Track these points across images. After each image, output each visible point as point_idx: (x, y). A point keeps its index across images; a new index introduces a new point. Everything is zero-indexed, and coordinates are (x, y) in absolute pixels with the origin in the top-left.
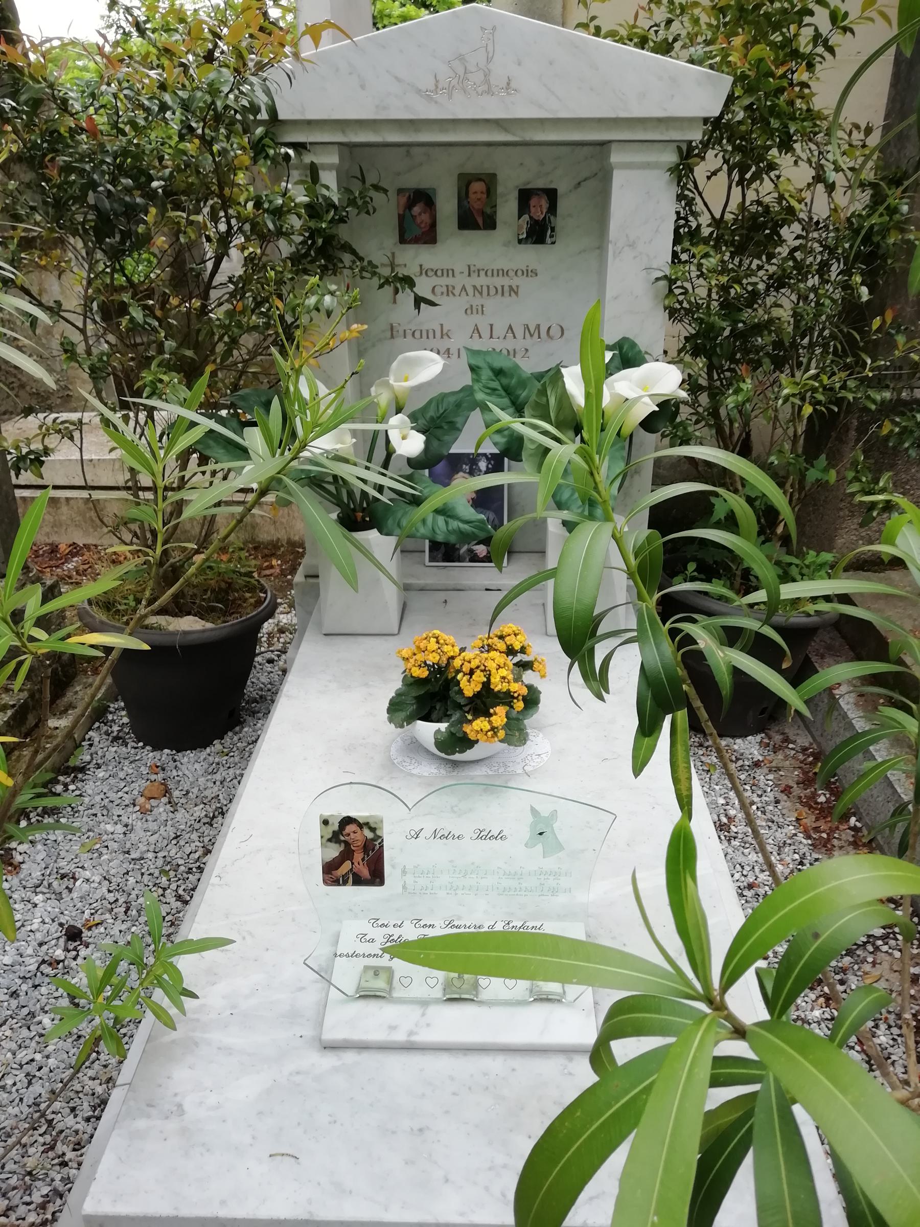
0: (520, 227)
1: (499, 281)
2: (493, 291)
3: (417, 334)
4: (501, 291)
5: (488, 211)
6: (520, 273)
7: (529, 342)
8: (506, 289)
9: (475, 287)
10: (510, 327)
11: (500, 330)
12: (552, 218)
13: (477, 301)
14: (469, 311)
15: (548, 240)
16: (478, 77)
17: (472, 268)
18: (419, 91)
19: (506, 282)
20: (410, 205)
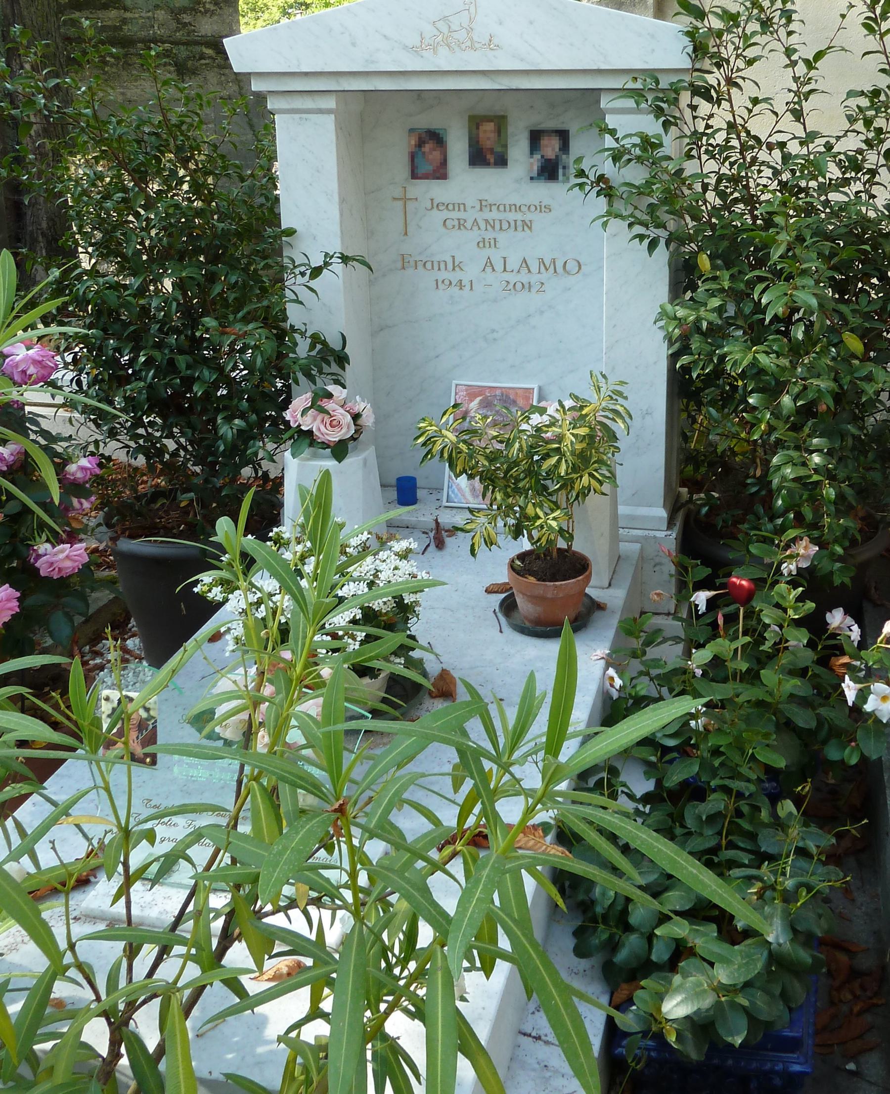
0: (532, 164)
1: (512, 216)
2: (505, 226)
3: (429, 265)
4: (515, 226)
5: (499, 149)
6: (533, 208)
7: (544, 276)
8: (519, 223)
9: (487, 221)
10: (525, 260)
11: (514, 263)
12: (564, 157)
13: (490, 235)
14: (481, 245)
15: (561, 177)
16: (462, 35)
17: (484, 203)
18: (405, 47)
19: (519, 216)
20: (421, 144)
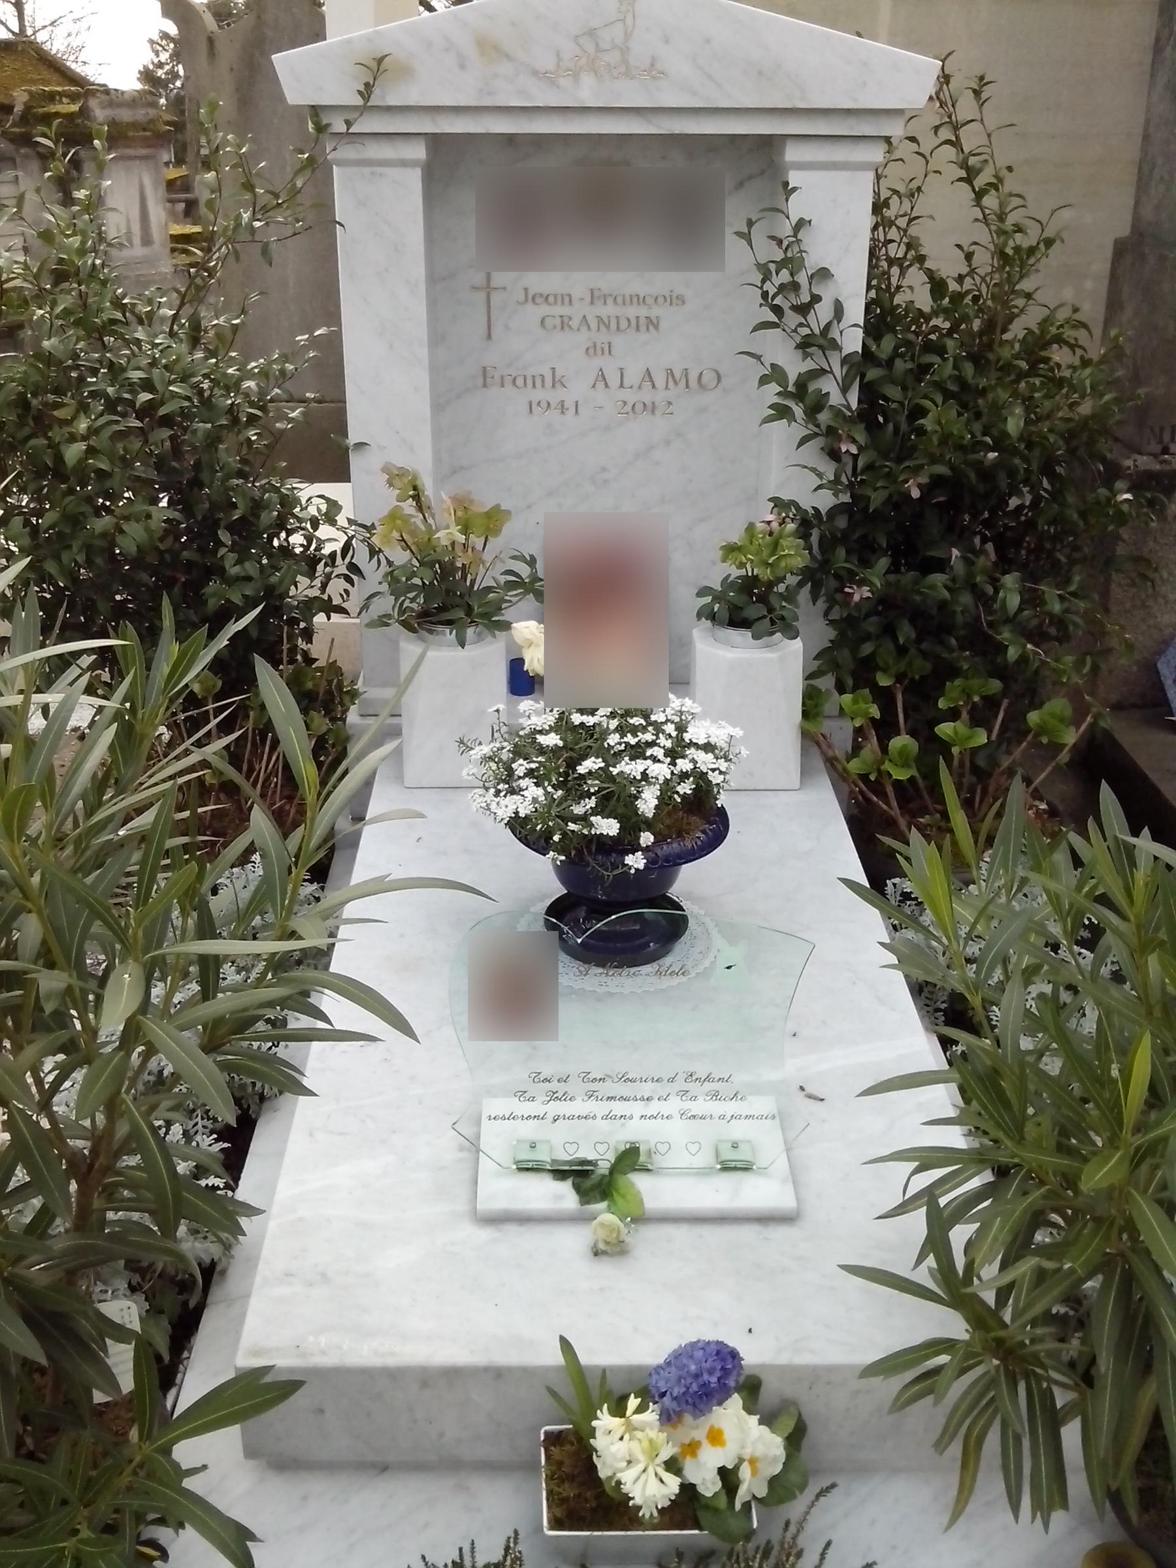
1: (632, 311)
3: (520, 382)
6: (661, 300)
8: (643, 321)
13: (603, 338)
14: (591, 351)
16: (613, 58)
17: (596, 293)
18: (535, 73)
19: (643, 312)
